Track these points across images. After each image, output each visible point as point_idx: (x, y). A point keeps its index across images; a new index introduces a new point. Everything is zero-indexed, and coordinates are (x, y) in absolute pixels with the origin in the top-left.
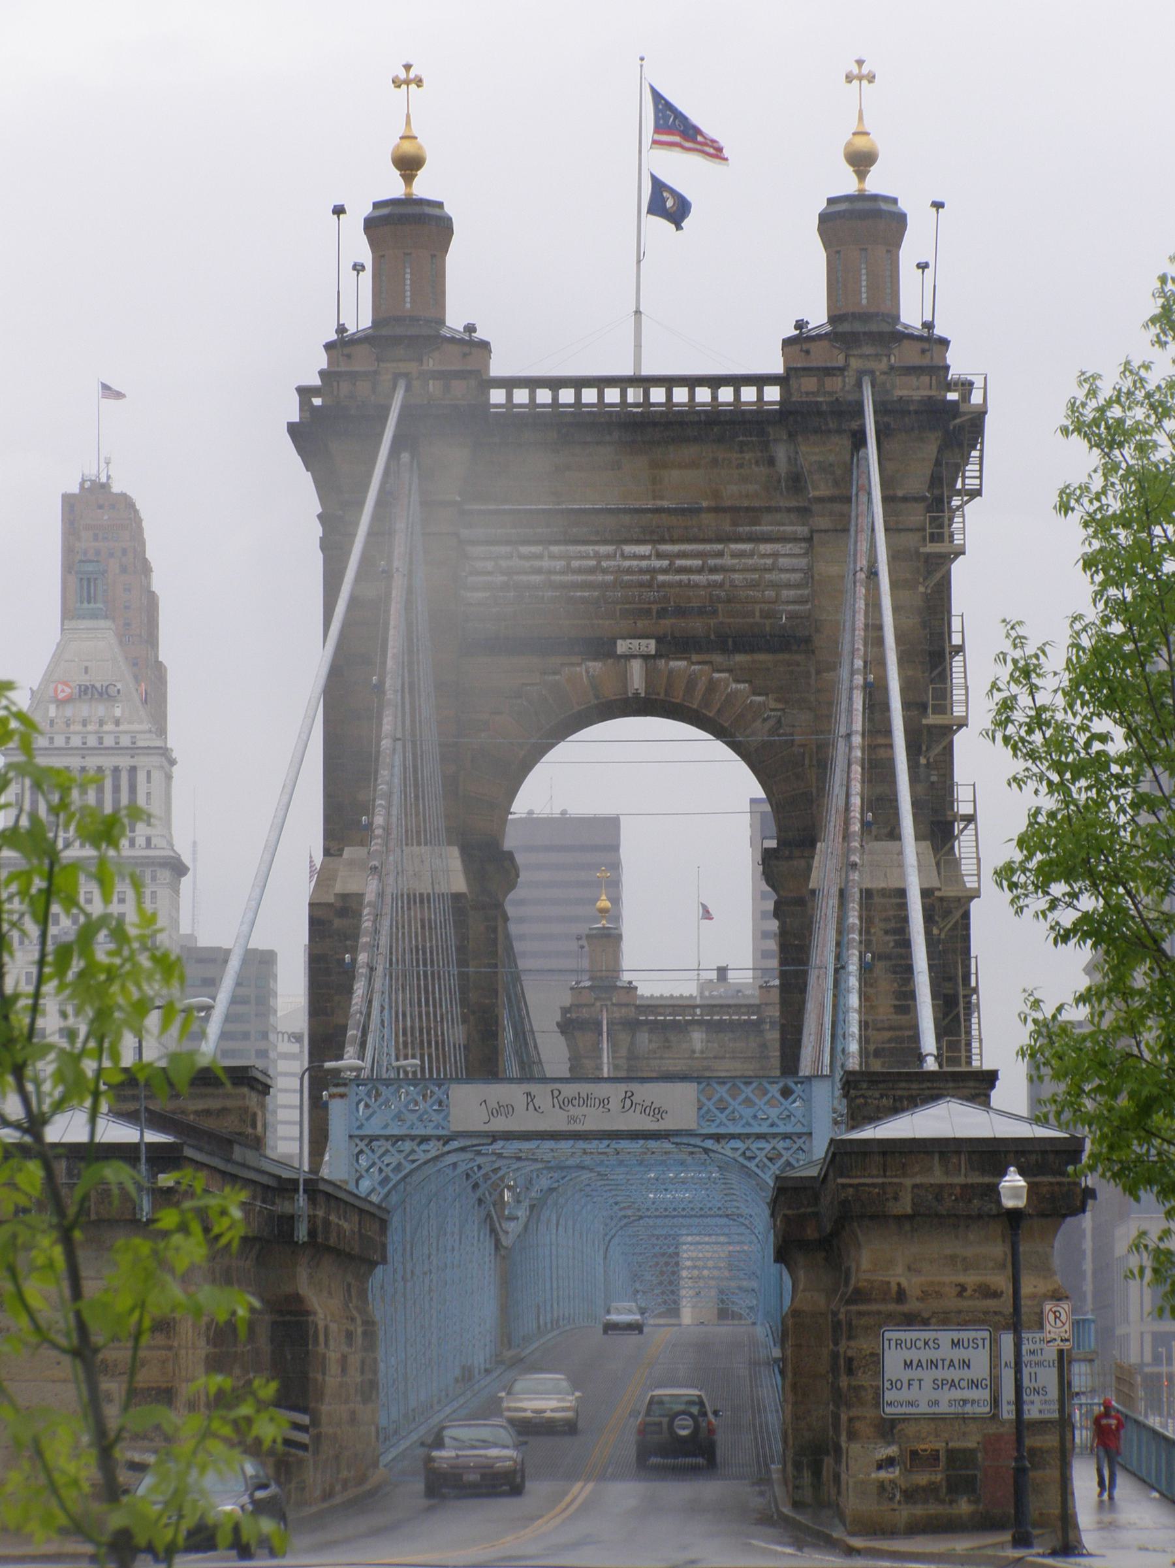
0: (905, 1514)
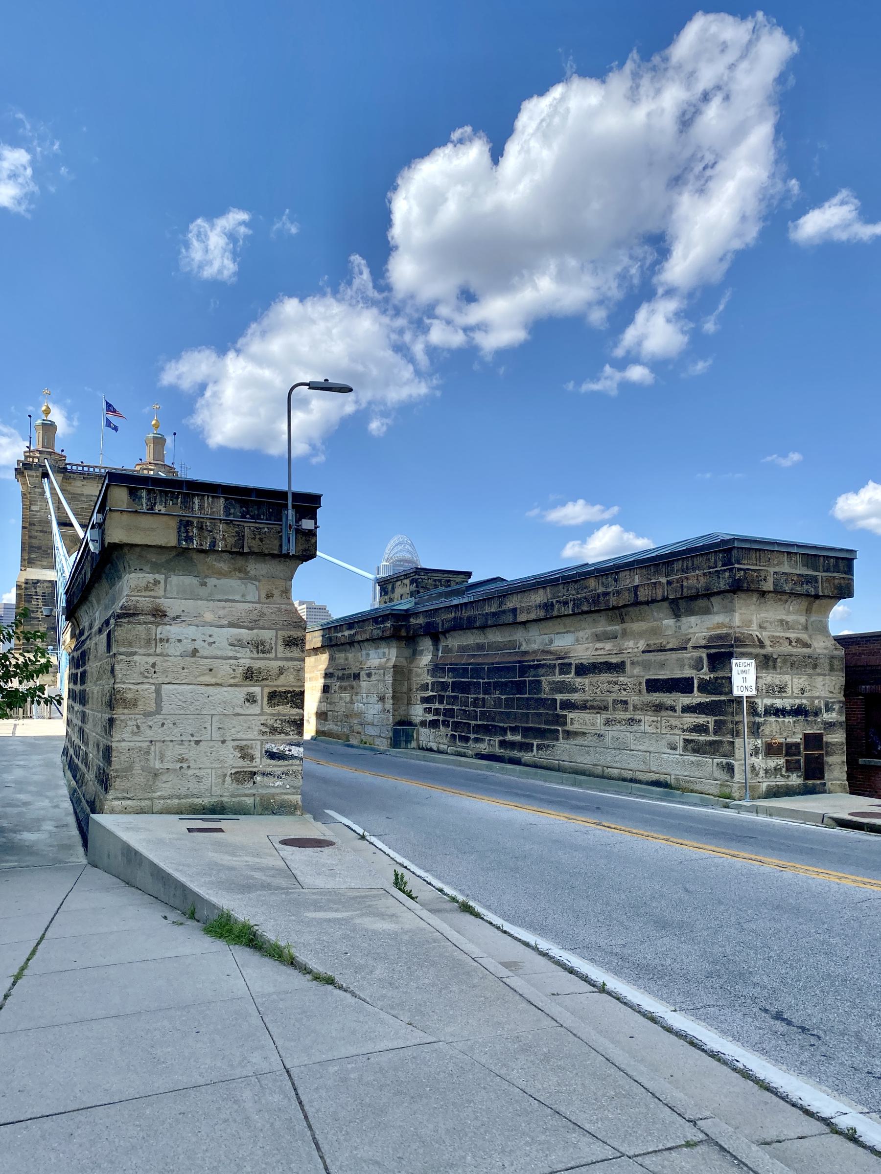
0: (764, 785)
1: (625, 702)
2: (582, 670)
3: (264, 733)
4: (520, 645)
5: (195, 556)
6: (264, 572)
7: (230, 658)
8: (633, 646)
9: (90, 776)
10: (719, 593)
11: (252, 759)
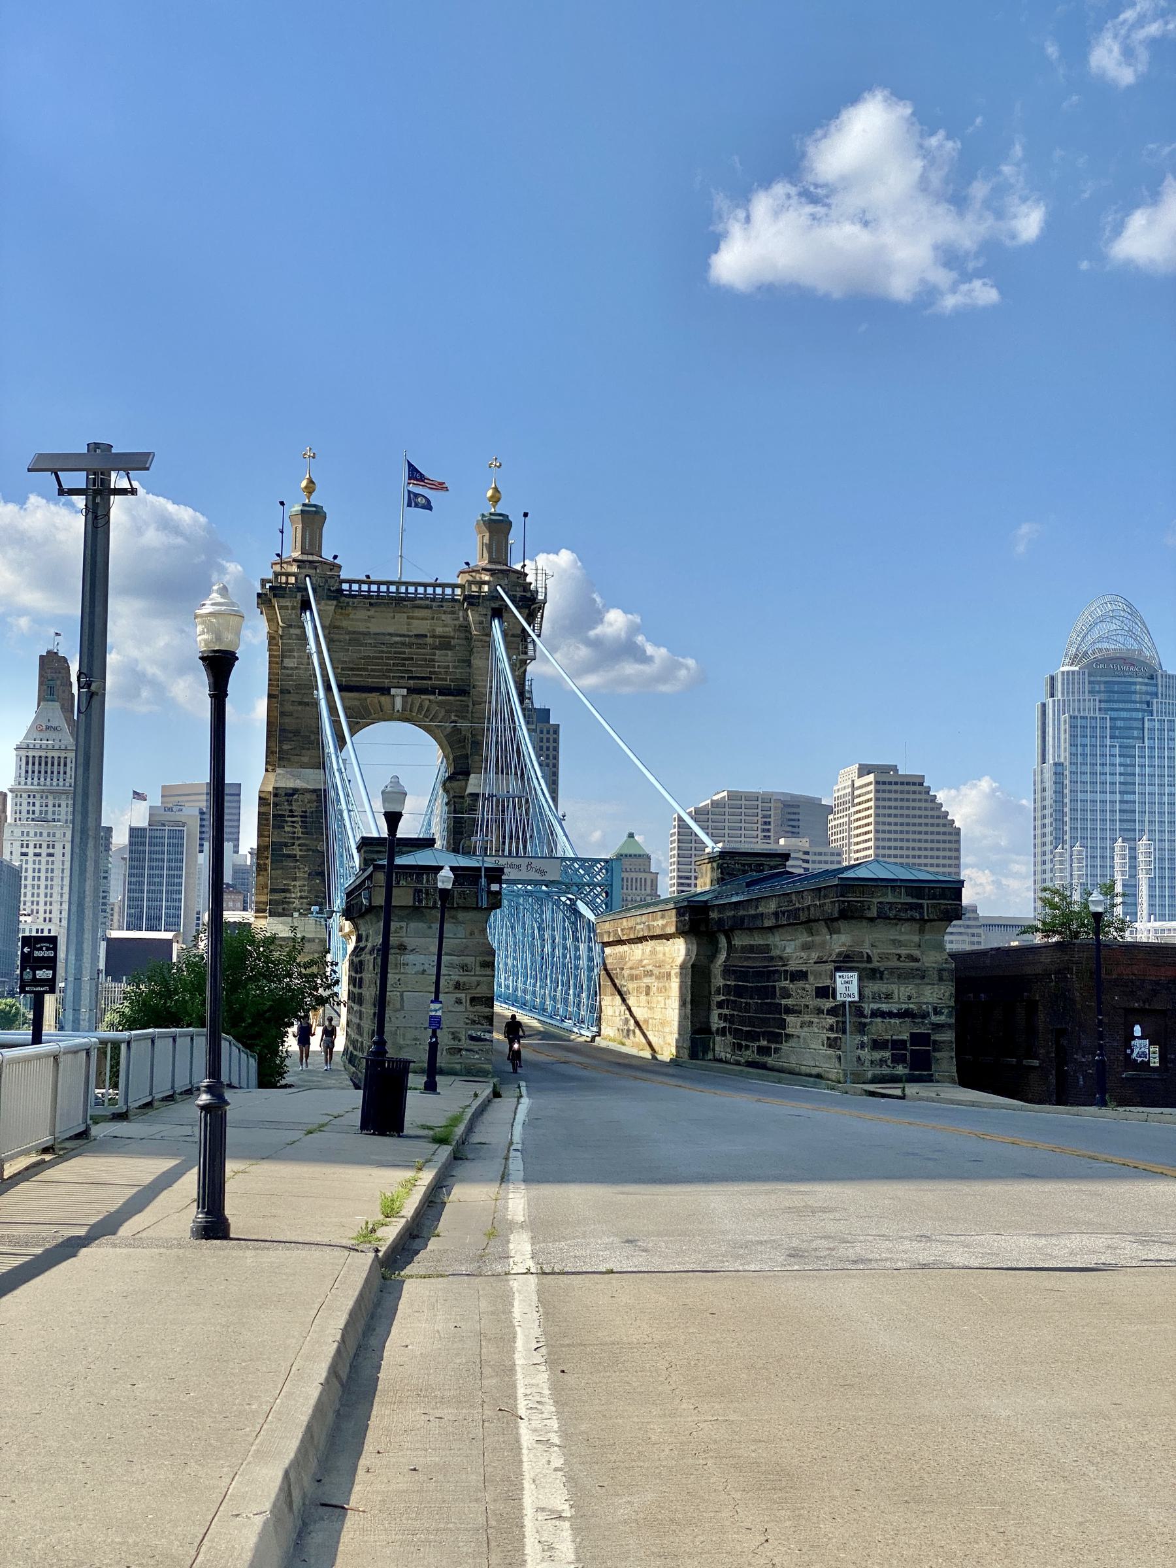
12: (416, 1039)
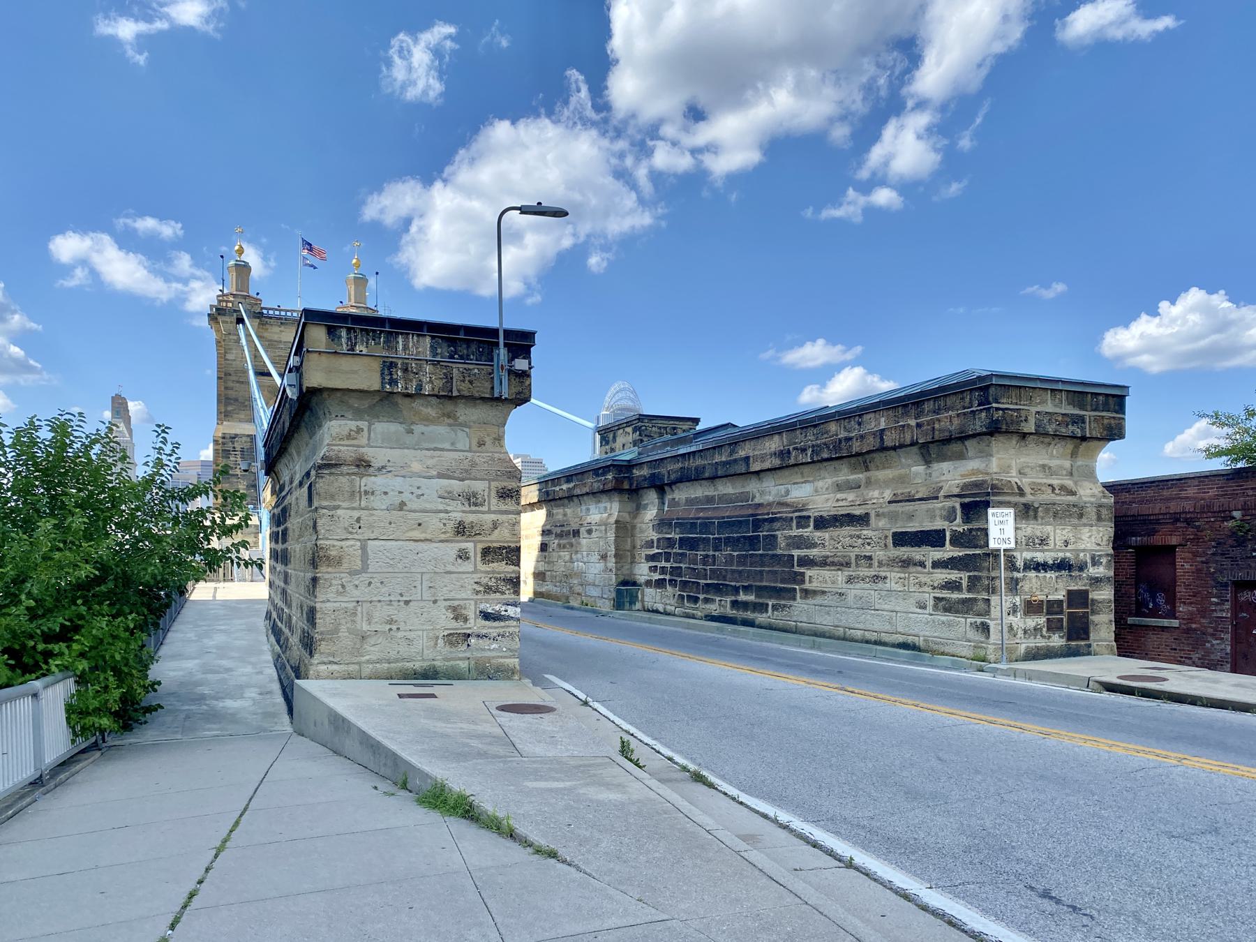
0: (1024, 646)
1: (870, 558)
2: (821, 523)
3: (478, 592)
4: (754, 497)
5: (400, 400)
6: (474, 418)
7: (440, 511)
8: (878, 496)
9: (294, 640)
10: (974, 436)
11: (466, 620)
12: (391, 622)
